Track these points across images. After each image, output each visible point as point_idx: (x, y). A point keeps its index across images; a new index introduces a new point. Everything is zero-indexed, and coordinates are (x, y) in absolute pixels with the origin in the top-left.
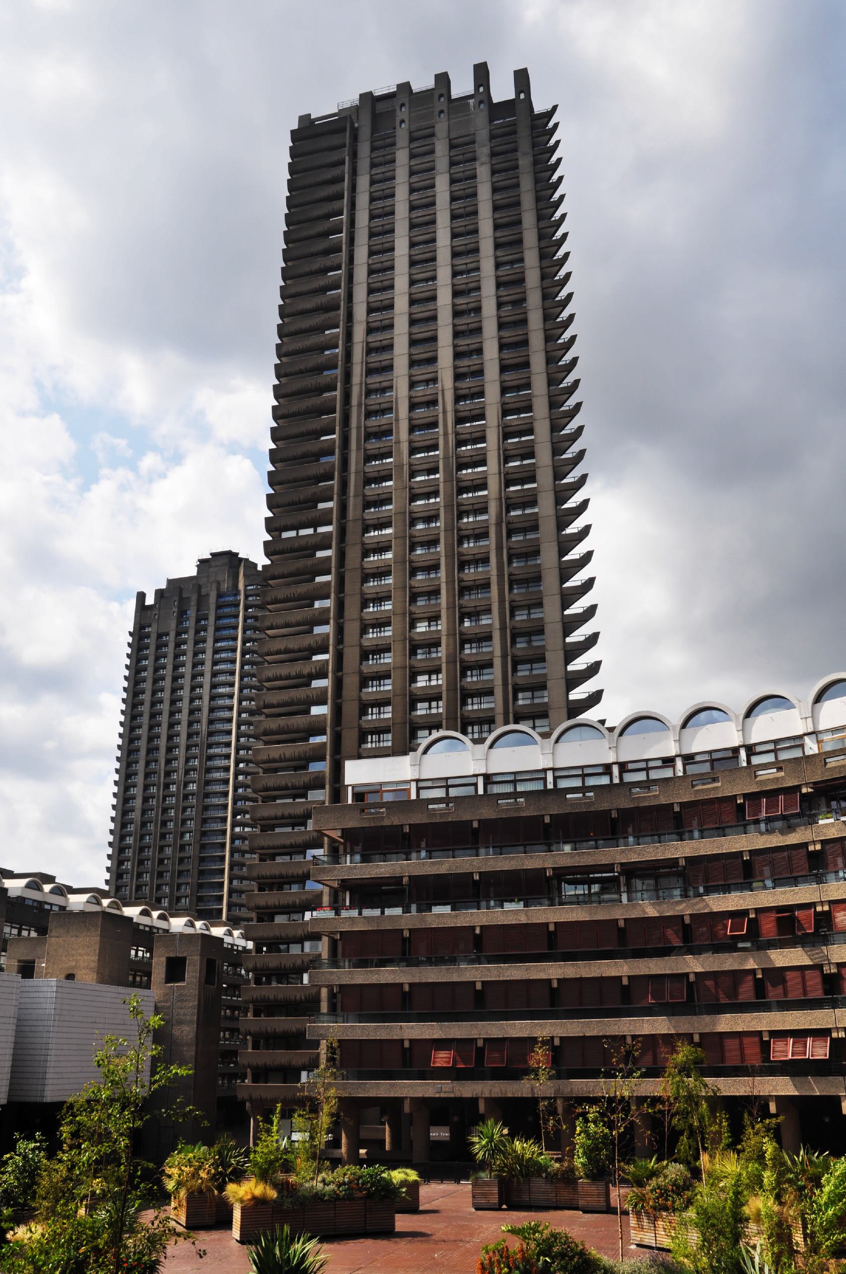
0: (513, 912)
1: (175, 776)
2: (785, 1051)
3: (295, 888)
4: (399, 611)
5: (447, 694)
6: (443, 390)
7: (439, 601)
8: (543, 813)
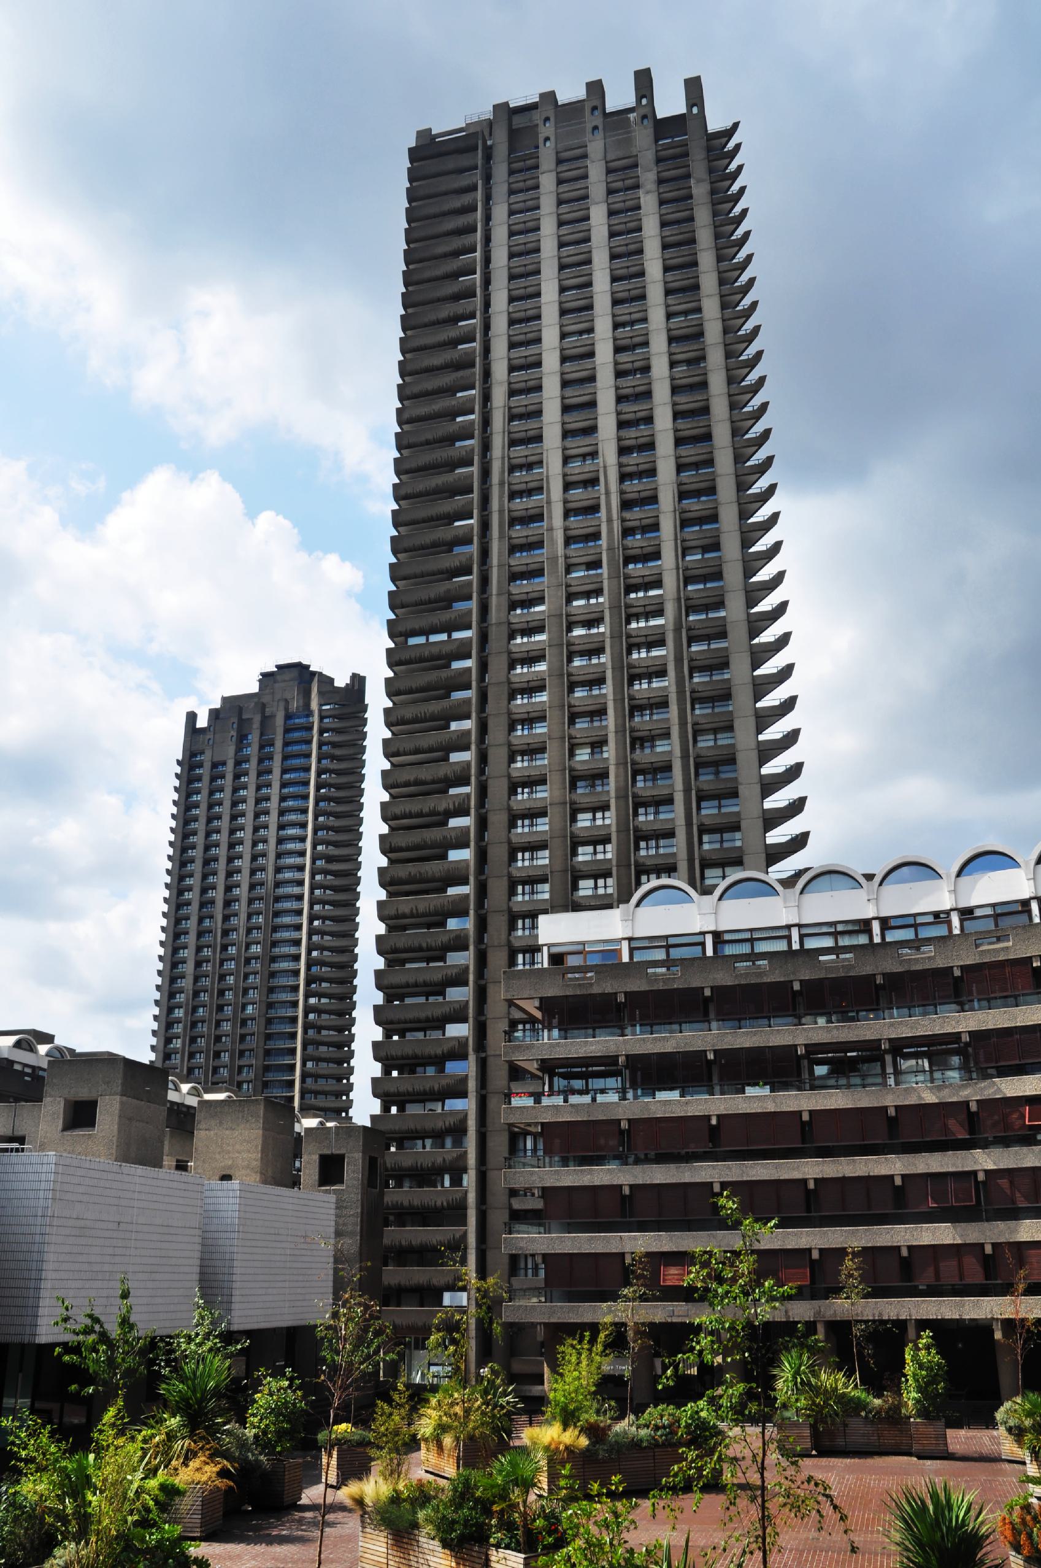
0: (758, 1098)
3: (431, 1071)
5: (618, 837)
6: (605, 467)
7: (604, 723)
8: (792, 978)
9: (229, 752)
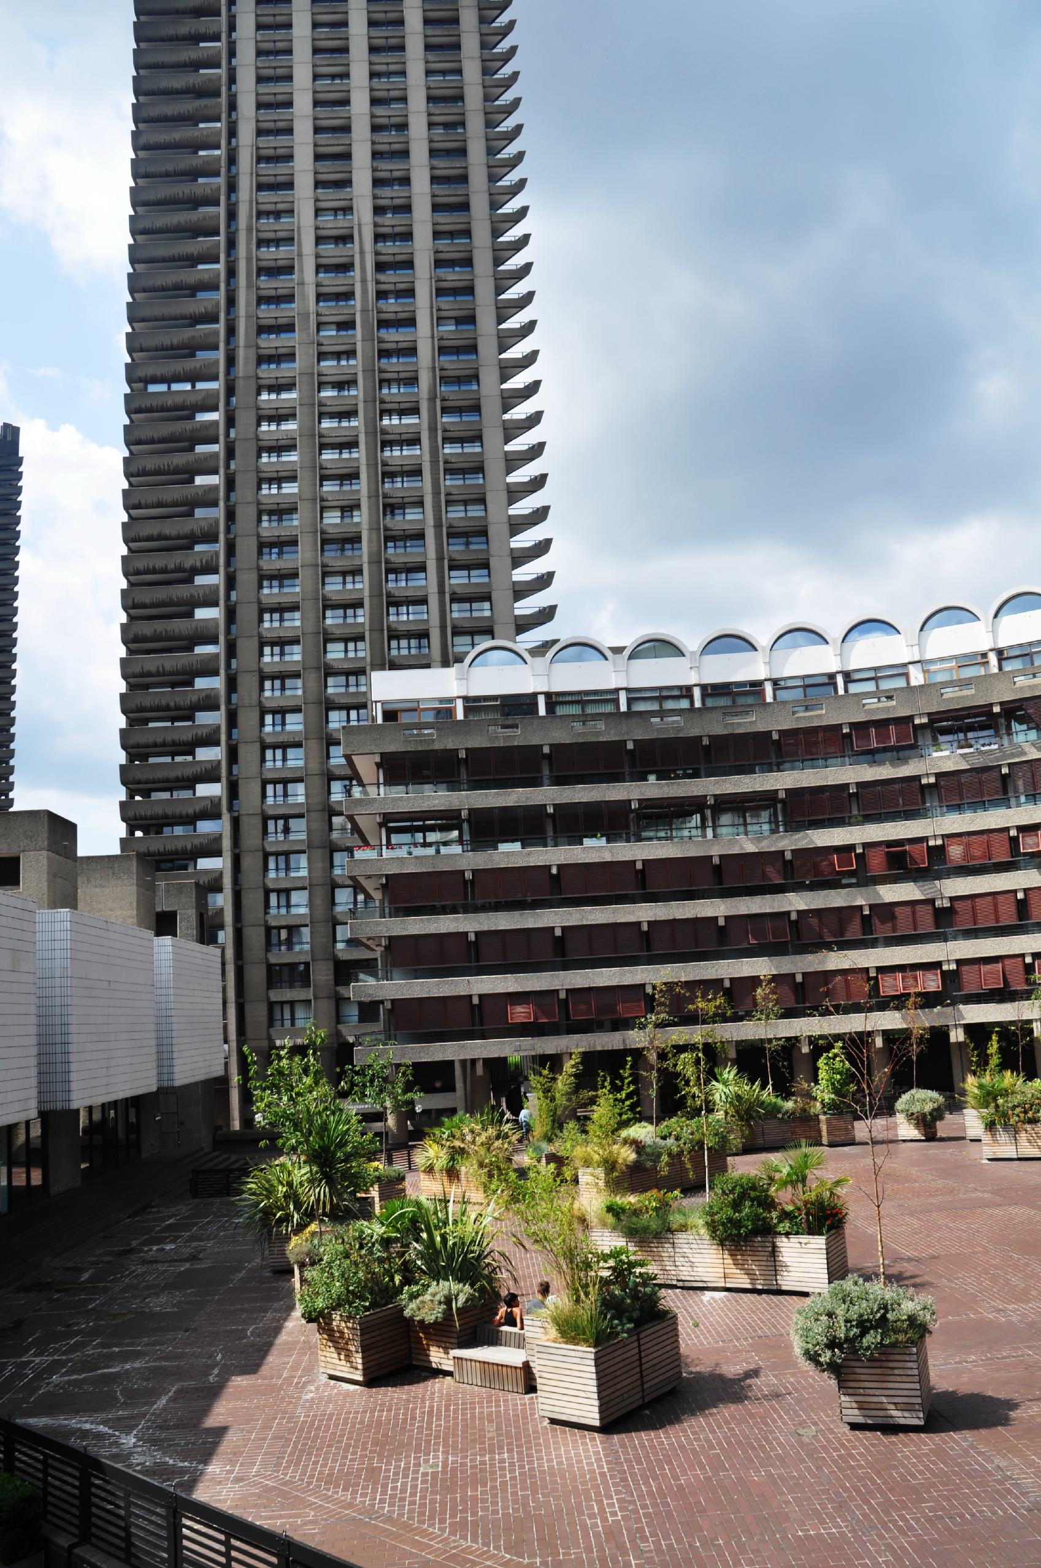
0: (595, 849)
2: (891, 986)
3: (179, 830)
4: (308, 495)
6: (360, 225)
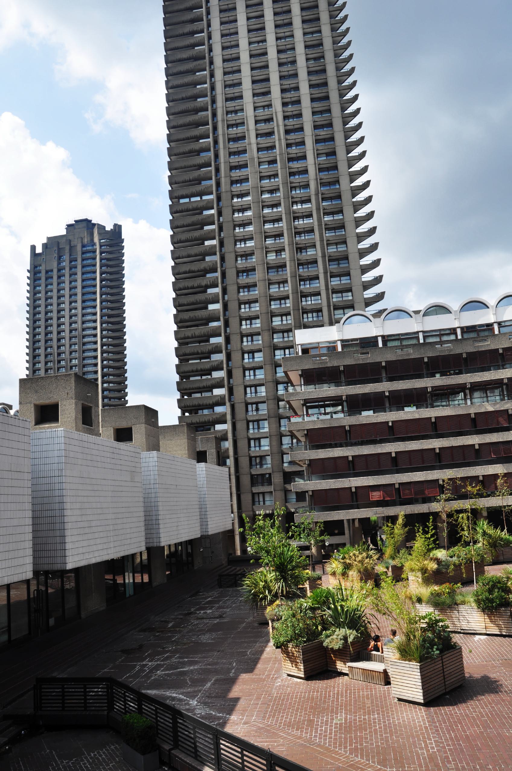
0: (410, 412)
1: (63, 356)
3: (206, 412)
4: (259, 246)
6: (276, 113)
9: (54, 265)
